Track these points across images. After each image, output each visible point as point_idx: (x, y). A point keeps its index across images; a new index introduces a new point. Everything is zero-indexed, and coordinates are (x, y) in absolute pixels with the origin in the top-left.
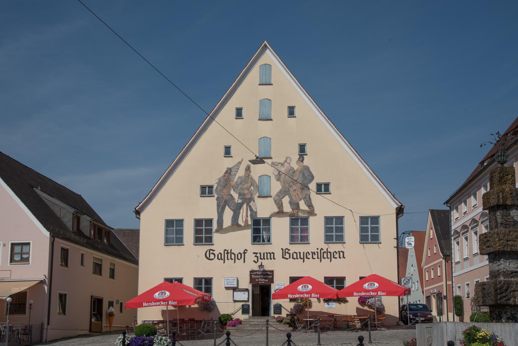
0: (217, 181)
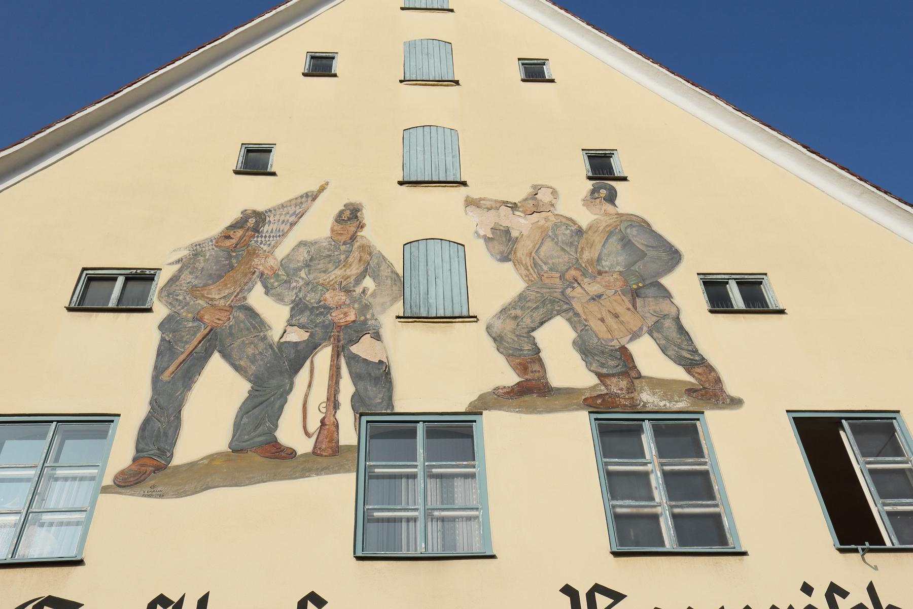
0: (185, 253)
